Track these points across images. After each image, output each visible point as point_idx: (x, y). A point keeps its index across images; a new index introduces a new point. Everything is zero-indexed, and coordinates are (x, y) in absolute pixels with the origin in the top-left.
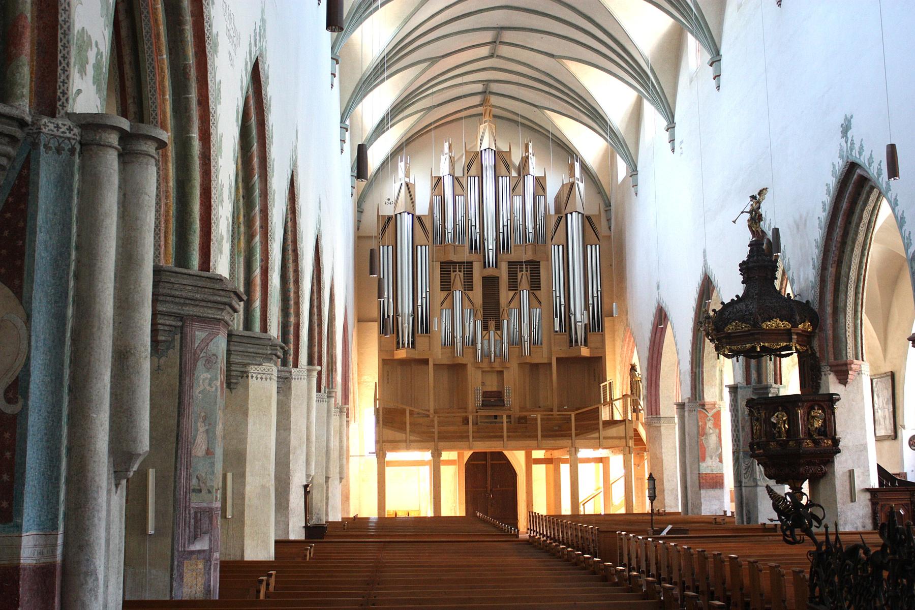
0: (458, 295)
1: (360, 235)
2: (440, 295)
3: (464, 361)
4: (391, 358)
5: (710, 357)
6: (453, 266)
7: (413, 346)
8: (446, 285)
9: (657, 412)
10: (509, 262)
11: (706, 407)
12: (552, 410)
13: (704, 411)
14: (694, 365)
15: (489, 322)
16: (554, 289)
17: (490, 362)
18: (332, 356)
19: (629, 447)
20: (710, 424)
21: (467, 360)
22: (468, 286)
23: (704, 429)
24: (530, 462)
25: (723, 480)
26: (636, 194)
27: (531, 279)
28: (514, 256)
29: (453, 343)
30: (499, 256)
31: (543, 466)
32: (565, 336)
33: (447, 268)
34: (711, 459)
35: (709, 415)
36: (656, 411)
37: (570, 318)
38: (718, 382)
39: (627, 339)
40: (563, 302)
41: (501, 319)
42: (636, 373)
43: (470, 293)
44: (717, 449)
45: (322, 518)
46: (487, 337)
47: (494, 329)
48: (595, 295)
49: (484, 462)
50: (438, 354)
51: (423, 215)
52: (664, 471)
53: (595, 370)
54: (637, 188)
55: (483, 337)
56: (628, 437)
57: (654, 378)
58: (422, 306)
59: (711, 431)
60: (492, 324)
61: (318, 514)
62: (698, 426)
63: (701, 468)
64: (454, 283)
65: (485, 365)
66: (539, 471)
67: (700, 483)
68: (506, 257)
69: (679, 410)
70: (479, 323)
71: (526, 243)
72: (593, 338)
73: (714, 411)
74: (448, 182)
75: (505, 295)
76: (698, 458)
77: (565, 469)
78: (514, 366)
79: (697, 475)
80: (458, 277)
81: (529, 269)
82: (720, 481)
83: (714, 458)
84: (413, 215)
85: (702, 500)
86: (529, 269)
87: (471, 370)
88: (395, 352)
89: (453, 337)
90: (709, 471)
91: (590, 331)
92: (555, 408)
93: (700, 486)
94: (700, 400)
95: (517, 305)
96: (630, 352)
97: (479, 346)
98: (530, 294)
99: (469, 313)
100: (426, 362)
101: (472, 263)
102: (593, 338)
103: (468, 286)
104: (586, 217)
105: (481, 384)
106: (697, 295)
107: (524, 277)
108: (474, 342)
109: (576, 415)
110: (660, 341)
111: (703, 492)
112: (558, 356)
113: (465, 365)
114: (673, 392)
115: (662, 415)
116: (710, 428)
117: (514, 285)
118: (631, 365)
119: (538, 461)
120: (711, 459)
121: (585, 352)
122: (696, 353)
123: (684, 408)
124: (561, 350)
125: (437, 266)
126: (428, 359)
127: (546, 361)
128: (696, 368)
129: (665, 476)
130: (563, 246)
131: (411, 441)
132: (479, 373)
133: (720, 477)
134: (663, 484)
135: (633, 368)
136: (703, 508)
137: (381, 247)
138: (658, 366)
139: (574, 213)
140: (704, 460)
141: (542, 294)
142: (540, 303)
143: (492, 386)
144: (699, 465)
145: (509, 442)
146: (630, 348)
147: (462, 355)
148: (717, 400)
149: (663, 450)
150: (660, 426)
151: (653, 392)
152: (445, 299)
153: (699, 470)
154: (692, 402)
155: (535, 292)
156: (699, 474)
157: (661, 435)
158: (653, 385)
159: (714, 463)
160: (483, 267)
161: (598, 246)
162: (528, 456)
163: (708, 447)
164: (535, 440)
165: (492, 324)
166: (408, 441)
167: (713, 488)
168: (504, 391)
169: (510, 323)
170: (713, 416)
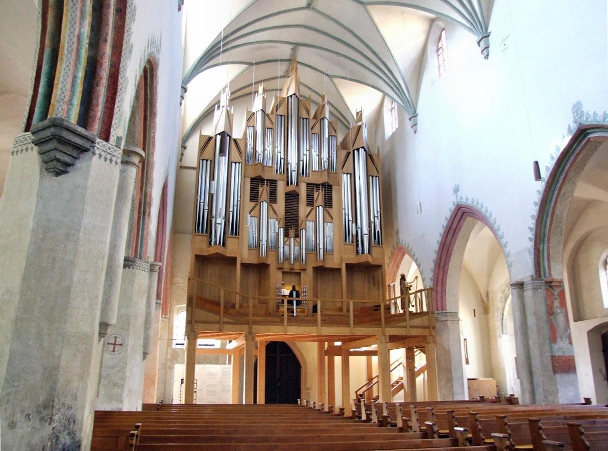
1: (182, 165)
2: (249, 205)
5: (556, 232)
6: (261, 182)
8: (254, 196)
10: (308, 184)
17: (290, 263)
21: (271, 261)
22: (273, 198)
25: (574, 363)
26: (415, 132)
28: (312, 179)
29: (258, 245)
30: (299, 178)
33: (257, 181)
34: (562, 340)
35: (556, 293)
40: (350, 218)
41: (300, 229)
42: (406, 282)
43: (273, 205)
45: (79, 417)
50: (246, 256)
51: (238, 139)
52: (452, 361)
53: (374, 277)
55: (284, 243)
56: (431, 327)
58: (233, 212)
61: (69, 408)
64: (262, 194)
68: (305, 180)
72: (374, 250)
74: (259, 117)
75: (303, 209)
79: (550, 358)
80: (264, 191)
83: (564, 339)
89: (259, 240)
90: (559, 354)
93: (554, 370)
94: (545, 277)
96: (395, 267)
100: (233, 260)
101: (276, 181)
108: (277, 247)
111: (558, 376)
112: (347, 262)
116: (557, 307)
117: (310, 201)
120: (562, 340)
125: (248, 181)
126: (236, 258)
127: (337, 267)
128: (540, 245)
129: (453, 365)
130: (351, 174)
131: (225, 323)
132: (280, 274)
136: (560, 394)
138: (446, 267)
141: (334, 211)
142: (332, 218)
144: (551, 348)
152: (255, 207)
154: (536, 280)
160: (286, 185)
163: (558, 326)
165: (292, 232)
166: (222, 322)
167: (566, 372)
169: (307, 233)
170: (558, 295)
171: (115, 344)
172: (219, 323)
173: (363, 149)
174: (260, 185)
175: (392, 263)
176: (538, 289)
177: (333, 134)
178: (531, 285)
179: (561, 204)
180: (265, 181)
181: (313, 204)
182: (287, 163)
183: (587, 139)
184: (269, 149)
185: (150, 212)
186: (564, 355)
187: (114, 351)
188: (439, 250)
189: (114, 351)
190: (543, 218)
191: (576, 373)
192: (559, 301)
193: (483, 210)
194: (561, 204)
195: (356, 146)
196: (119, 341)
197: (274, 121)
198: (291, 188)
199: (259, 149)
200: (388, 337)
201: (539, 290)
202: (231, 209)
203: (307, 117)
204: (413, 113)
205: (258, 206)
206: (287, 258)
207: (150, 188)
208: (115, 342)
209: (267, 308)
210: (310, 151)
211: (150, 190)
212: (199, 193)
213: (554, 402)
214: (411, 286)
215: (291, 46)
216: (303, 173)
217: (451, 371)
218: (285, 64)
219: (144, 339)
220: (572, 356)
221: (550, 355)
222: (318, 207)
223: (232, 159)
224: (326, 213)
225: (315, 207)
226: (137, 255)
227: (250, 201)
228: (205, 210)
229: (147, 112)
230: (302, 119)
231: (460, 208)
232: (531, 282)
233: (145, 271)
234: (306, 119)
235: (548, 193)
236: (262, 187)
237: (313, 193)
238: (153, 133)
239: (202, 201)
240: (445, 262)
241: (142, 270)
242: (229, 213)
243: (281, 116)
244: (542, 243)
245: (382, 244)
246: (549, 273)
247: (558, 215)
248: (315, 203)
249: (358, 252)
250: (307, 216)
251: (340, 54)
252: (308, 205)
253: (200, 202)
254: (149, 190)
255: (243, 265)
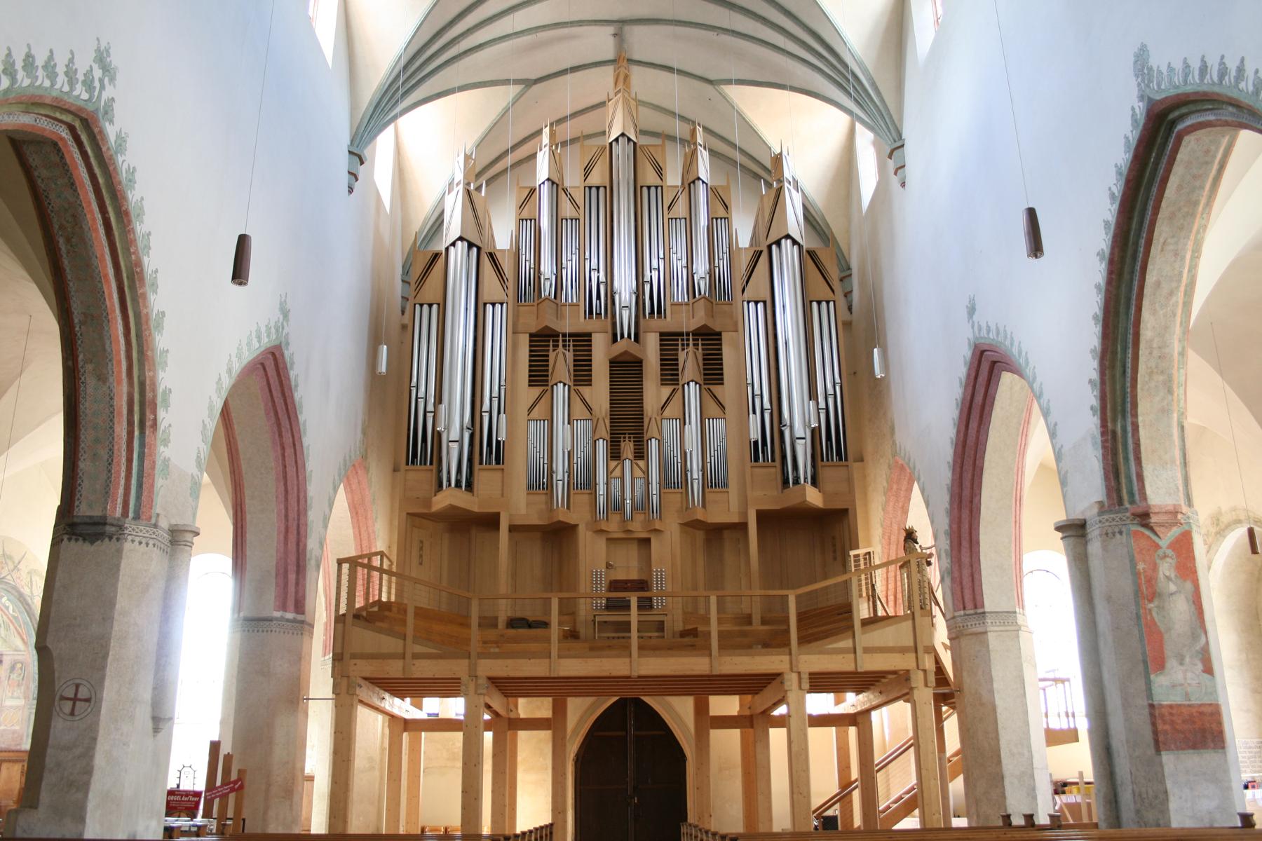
0: (560, 392)
2: (527, 394)
3: (571, 518)
4: (425, 511)
5: (1153, 384)
7: (470, 486)
8: (539, 375)
9: (977, 602)
10: (662, 334)
11: (1154, 519)
12: (750, 623)
13: (1147, 532)
14: (1109, 414)
15: (622, 444)
16: (749, 381)
18: (142, 385)
19: (925, 671)
20: (1166, 569)
21: (578, 515)
23: (1151, 581)
24: (707, 722)
26: (903, 185)
27: (704, 364)
28: (671, 322)
31: (736, 733)
32: (773, 470)
33: (543, 340)
34: (1181, 664)
35: (1164, 543)
36: (974, 599)
37: (782, 434)
38: (1177, 453)
39: (895, 487)
40: (767, 405)
41: (645, 439)
42: (917, 546)
43: (585, 391)
44: (1195, 637)
46: (617, 473)
47: (631, 456)
48: (830, 391)
49: (619, 733)
53: (834, 538)
54: (904, 172)
55: (609, 473)
57: (966, 526)
59: (1172, 588)
60: (628, 448)
62: (1136, 574)
63: (1156, 690)
65: (613, 526)
66: (727, 742)
67: (1155, 733)
69: (1072, 539)
70: (601, 445)
71: (694, 296)
72: (826, 473)
73: (1175, 532)
75: (653, 393)
76: (1145, 662)
77: (777, 736)
78: (671, 528)
79: (1146, 711)
80: (561, 361)
81: (700, 347)
82: (1214, 726)
83: (1187, 660)
84: (479, 249)
85: (1169, 785)
86: (700, 347)
87: (584, 535)
88: (434, 499)
89: (551, 472)
90: (1176, 698)
91: (822, 460)
92: (756, 619)
93: (1157, 742)
94: (1132, 502)
95: (679, 414)
97: (601, 489)
98: (704, 391)
99: (582, 427)
101: (589, 335)
102: (829, 474)
103: (582, 372)
104: (808, 252)
105: (604, 566)
106: (1121, 183)
107: (689, 360)
108: (591, 484)
109: (798, 597)
110: (978, 438)
111: (1167, 758)
113: (574, 528)
114: (1011, 557)
115: (989, 605)
116: (1168, 578)
117: (670, 372)
118: (906, 530)
119: (725, 722)
121: (814, 497)
122: (1113, 377)
123: (1083, 536)
124: (767, 496)
125: (524, 341)
126: (497, 515)
127: (735, 519)
128: (1114, 420)
130: (765, 302)
131: (416, 656)
132: (601, 543)
133: (1212, 714)
134: (999, 762)
135: (910, 536)
136: (1173, 805)
137: (418, 307)
138: (976, 500)
139: (783, 241)
140: (1160, 665)
141: (726, 392)
143: (628, 568)
145: (643, 660)
146: (901, 504)
147: (568, 507)
148: (1182, 503)
149: (995, 686)
150: (986, 633)
151: (966, 559)
153: (1150, 695)
154: (1110, 511)
155: (711, 387)
156: (1152, 706)
157: (988, 651)
158: (965, 544)
159: (1189, 675)
161: (831, 304)
162: (701, 709)
164: (702, 655)
165: (628, 448)
166: (408, 656)
168: (652, 580)
169: (664, 448)
170: (1172, 546)
171: (75, 699)
172: (403, 657)
173: (789, 241)
174: (551, 348)
175: (891, 504)
176: (1114, 534)
177: (721, 212)
178: (1100, 525)
179: (1154, 312)
180: (561, 338)
181: (678, 380)
182: (611, 295)
183: (1174, 135)
184: (570, 265)
185: (155, 420)
186: (1187, 703)
187: (72, 714)
188: (955, 461)
189: (72, 714)
190: (1114, 353)
191: (1223, 748)
192: (1173, 562)
193: (1015, 351)
194: (1154, 312)
195: (772, 238)
196: (83, 693)
197: (580, 201)
198: (622, 346)
199: (547, 268)
200: (805, 677)
201: (1118, 536)
202: (486, 407)
203: (658, 182)
204: (895, 141)
205: (549, 392)
206: (616, 506)
207: (150, 370)
208: (76, 694)
209: (575, 621)
210: (667, 259)
211: (151, 374)
212: (415, 379)
213: (1158, 825)
214: (931, 555)
215: (610, 30)
216: (652, 312)
217: (999, 756)
218: (610, 70)
219: (155, 689)
220: (1211, 705)
221: (1146, 703)
222: (688, 384)
223: (485, 297)
224: (706, 395)
225: (680, 387)
226: (128, 513)
227: (529, 385)
228: (428, 414)
229: (107, 212)
230: (645, 190)
231: (982, 352)
232: (1098, 518)
233: (147, 544)
234: (657, 187)
235: (1118, 287)
236: (554, 350)
237: (677, 355)
238: (134, 253)
239: (422, 394)
240: (972, 488)
241: (140, 543)
242: (481, 417)
243: (598, 188)
244: (1120, 417)
245: (846, 460)
246: (1139, 490)
247: (1151, 341)
248: (680, 377)
249: (785, 482)
250: (663, 407)
251: (719, 28)
252: (664, 382)
253: (417, 398)
254: (148, 374)
255: (513, 529)
